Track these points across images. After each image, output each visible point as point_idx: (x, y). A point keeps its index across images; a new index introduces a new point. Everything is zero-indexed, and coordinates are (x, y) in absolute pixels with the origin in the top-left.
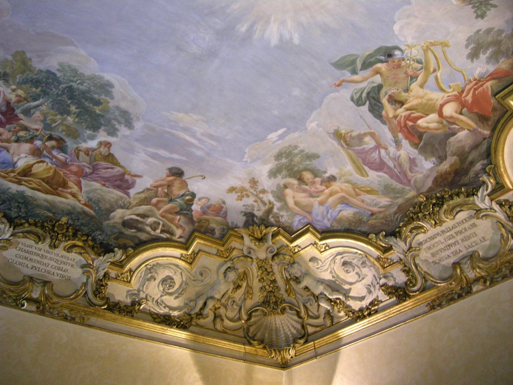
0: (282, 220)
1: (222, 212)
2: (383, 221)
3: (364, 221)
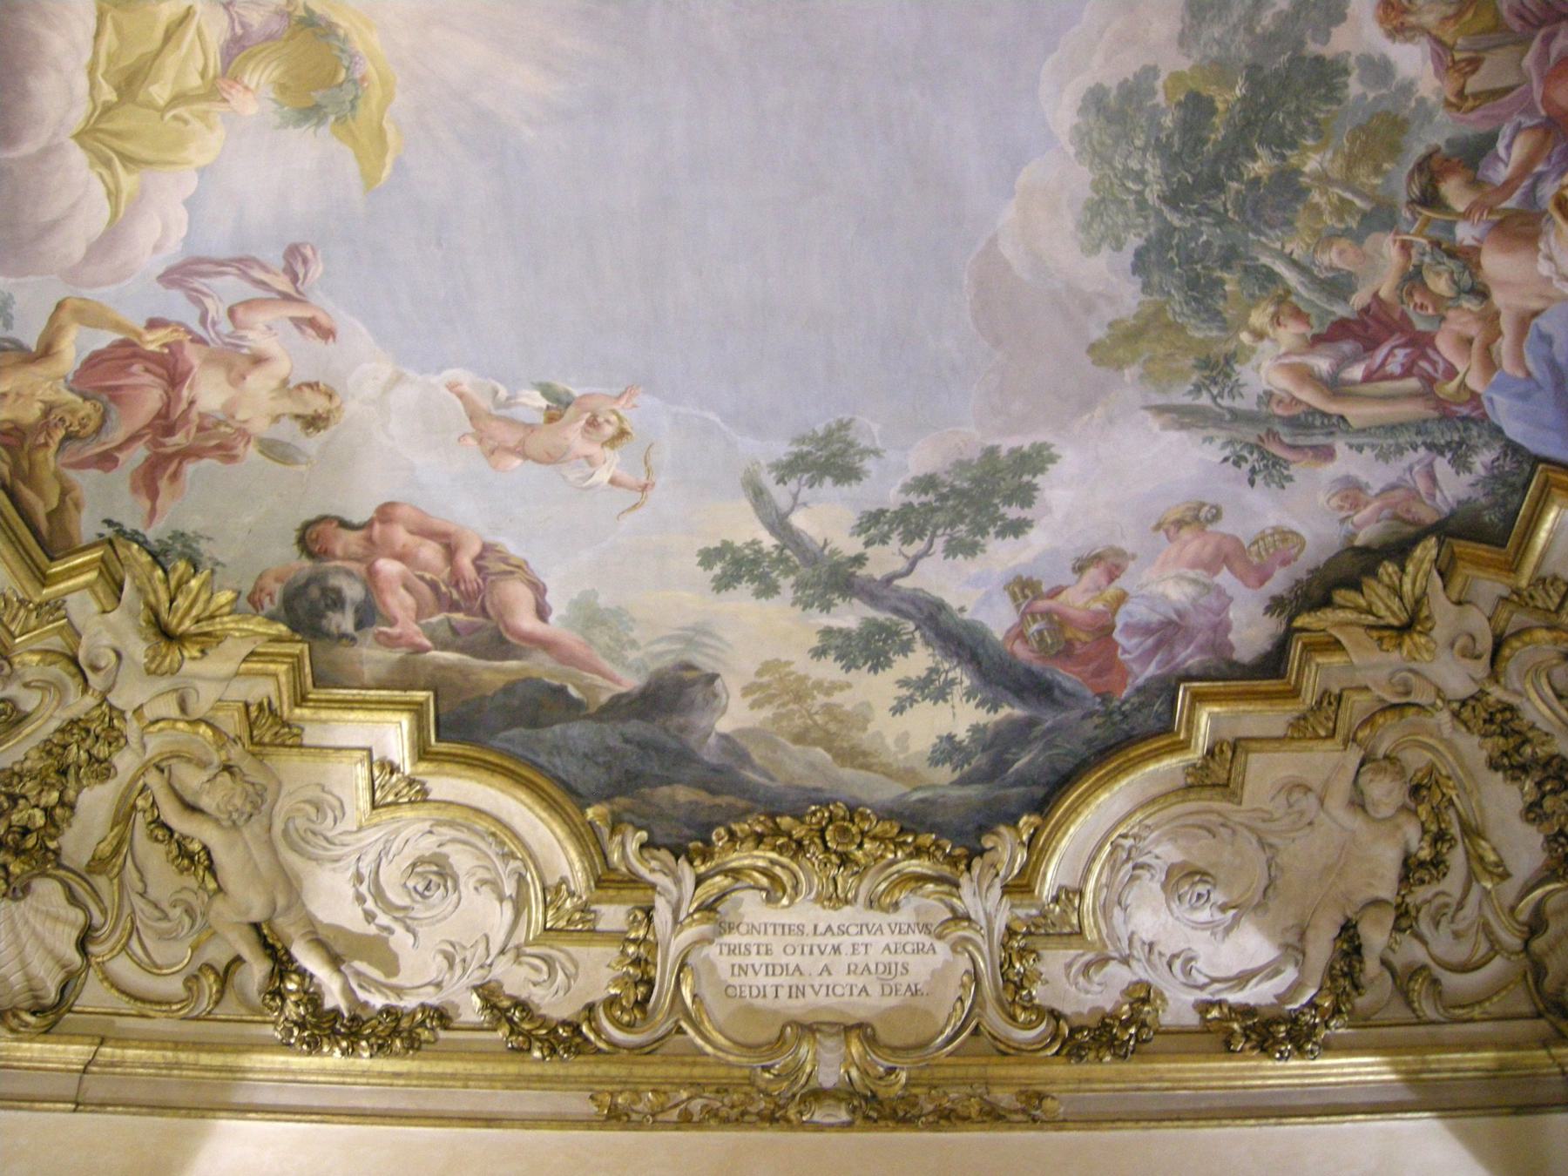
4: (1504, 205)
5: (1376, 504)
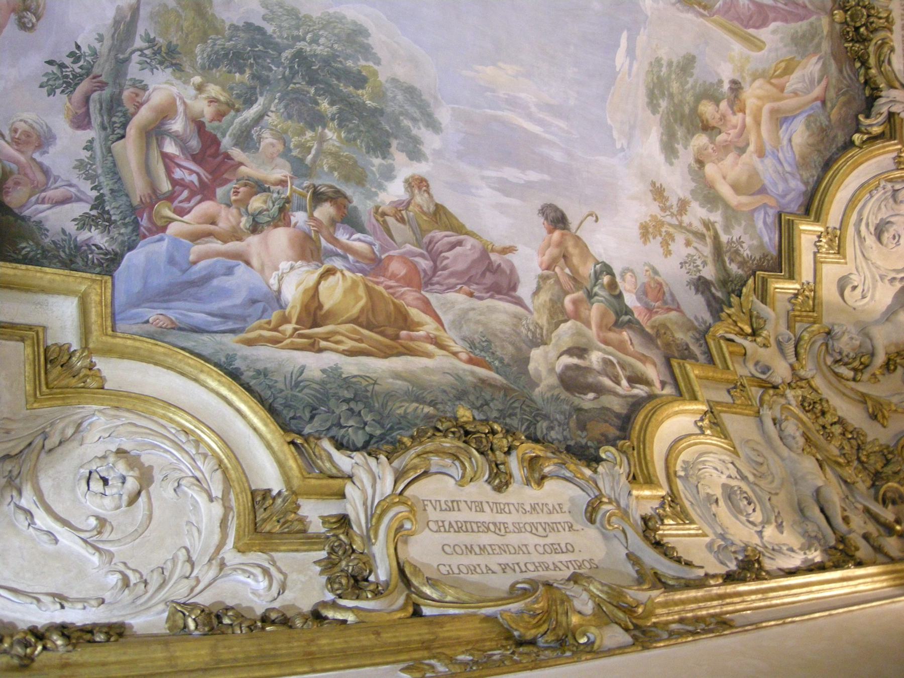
0: (746, 252)
1: (667, 295)
2: (842, 99)
3: (827, 126)
4: (322, 239)
5: (22, 158)
